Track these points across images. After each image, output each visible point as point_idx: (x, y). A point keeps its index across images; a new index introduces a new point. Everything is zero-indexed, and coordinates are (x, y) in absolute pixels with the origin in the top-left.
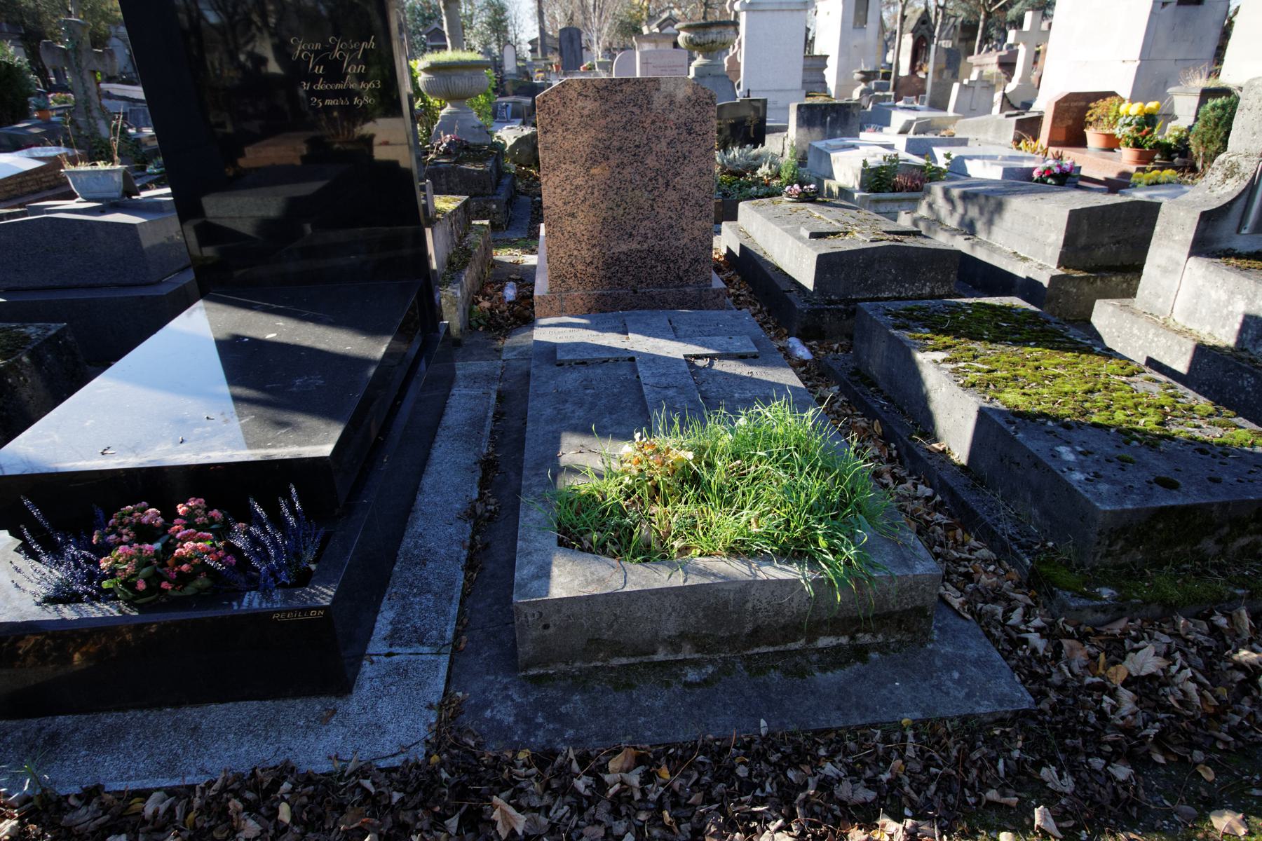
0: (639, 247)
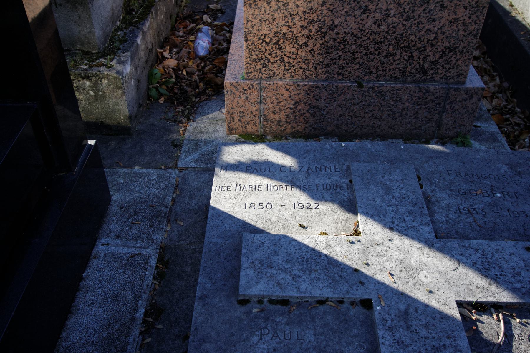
0: (375, 27)
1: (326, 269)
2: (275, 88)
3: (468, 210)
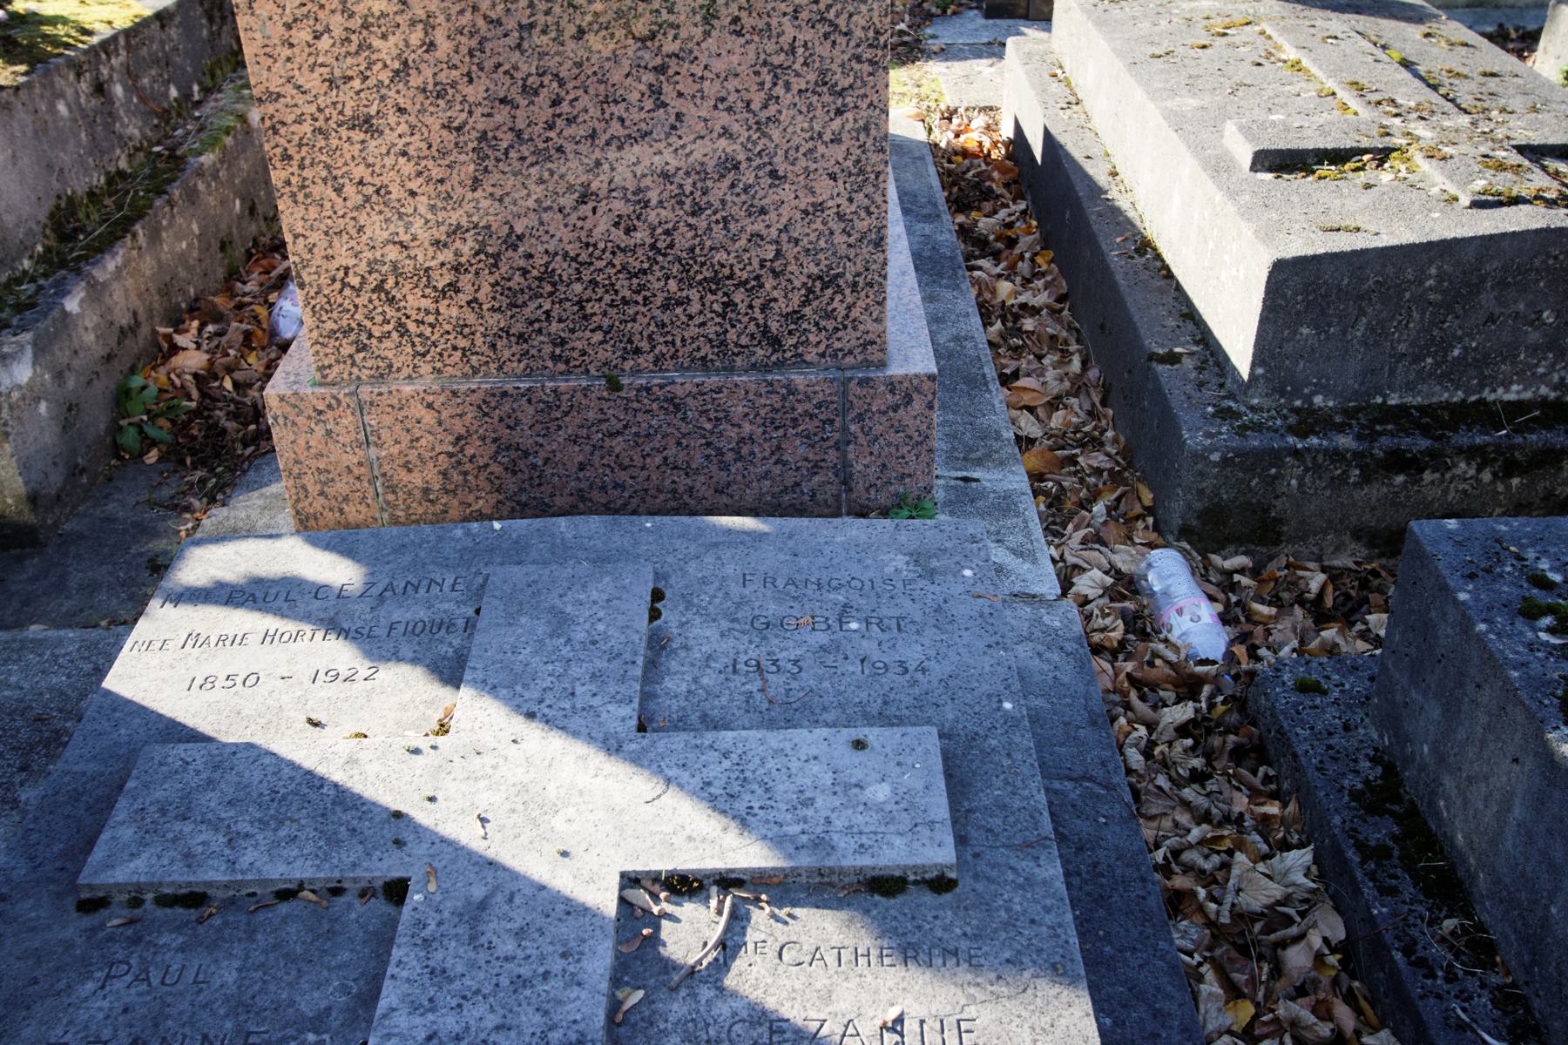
0: (618, 235)
1: (323, 815)
2: (395, 402)
3: (758, 665)
